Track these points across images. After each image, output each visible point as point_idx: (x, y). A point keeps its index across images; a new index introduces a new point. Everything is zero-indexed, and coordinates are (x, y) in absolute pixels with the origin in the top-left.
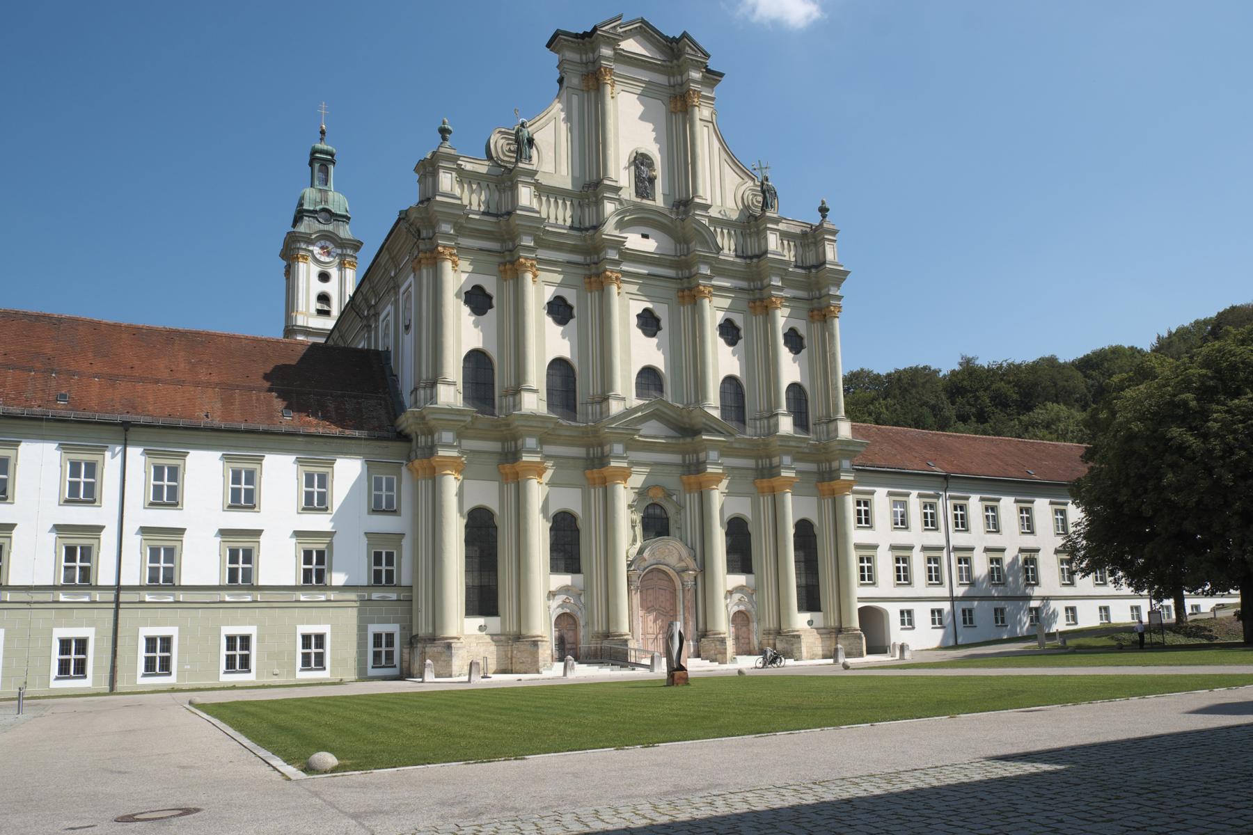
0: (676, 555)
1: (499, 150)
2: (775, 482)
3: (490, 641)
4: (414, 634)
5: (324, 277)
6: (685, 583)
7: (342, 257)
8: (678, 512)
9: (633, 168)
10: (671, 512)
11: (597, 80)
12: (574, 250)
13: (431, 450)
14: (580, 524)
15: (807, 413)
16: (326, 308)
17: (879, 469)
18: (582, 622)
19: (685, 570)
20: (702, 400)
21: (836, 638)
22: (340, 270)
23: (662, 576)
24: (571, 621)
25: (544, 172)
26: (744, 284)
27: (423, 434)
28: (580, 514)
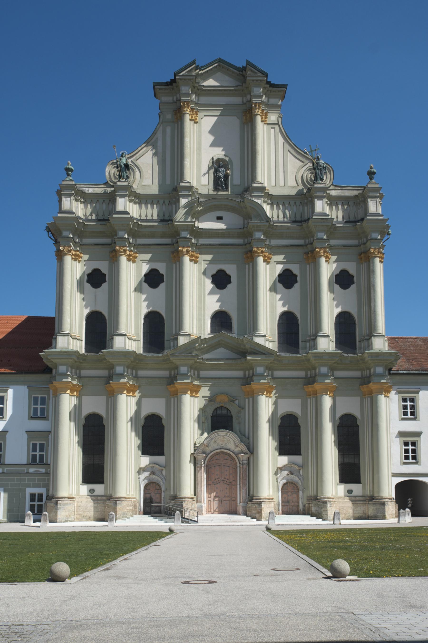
1: (112, 176)
2: (317, 386)
3: (91, 500)
6: (241, 462)
9: (211, 171)
10: (234, 411)
12: (163, 235)
14: (164, 422)
15: (355, 333)
17: (424, 372)
18: (163, 489)
20: (254, 330)
23: (227, 457)
24: (158, 488)
25: (144, 185)
26: (300, 242)
28: (165, 417)
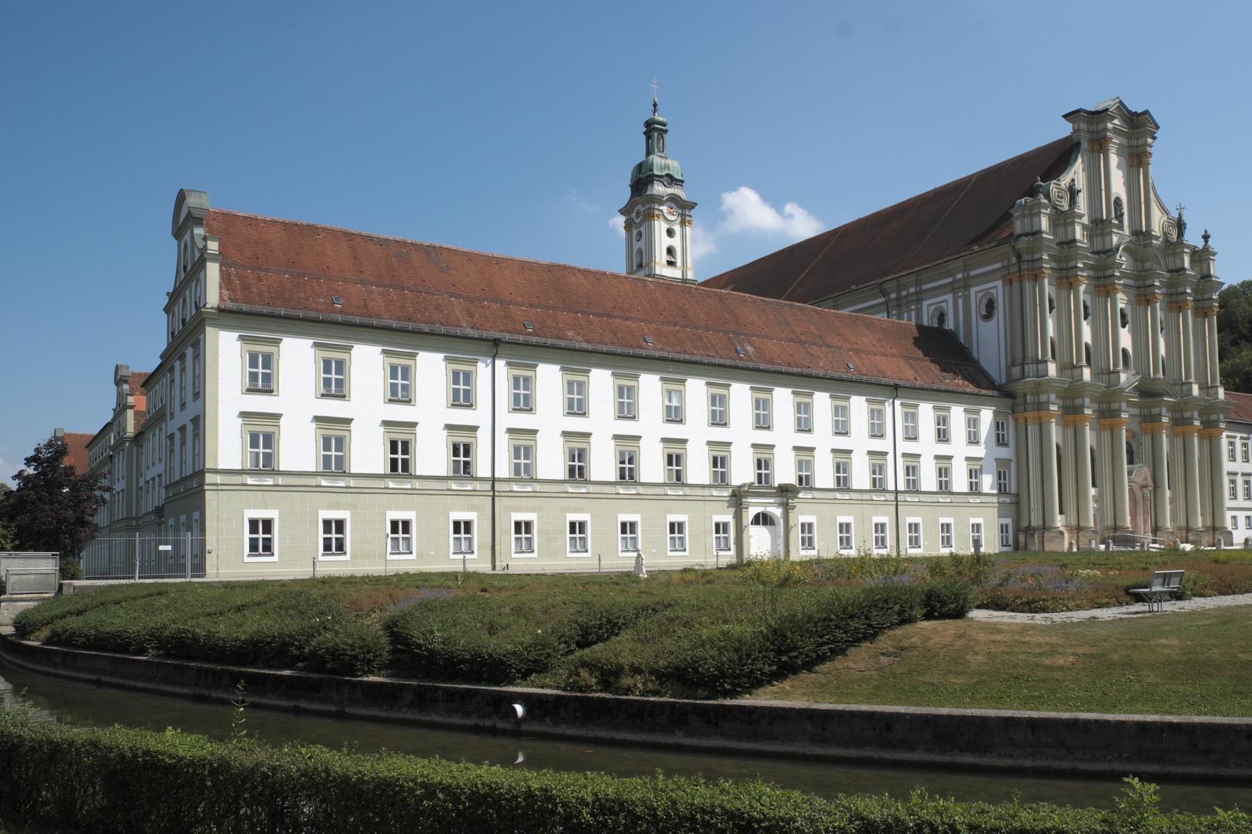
0: (1143, 476)
4: (1024, 524)
5: (670, 233)
7: (683, 216)
8: (1139, 448)
11: (1100, 145)
13: (1041, 406)
16: (673, 260)
19: (1145, 486)
21: (1214, 533)
22: (682, 226)
27: (1032, 394)
